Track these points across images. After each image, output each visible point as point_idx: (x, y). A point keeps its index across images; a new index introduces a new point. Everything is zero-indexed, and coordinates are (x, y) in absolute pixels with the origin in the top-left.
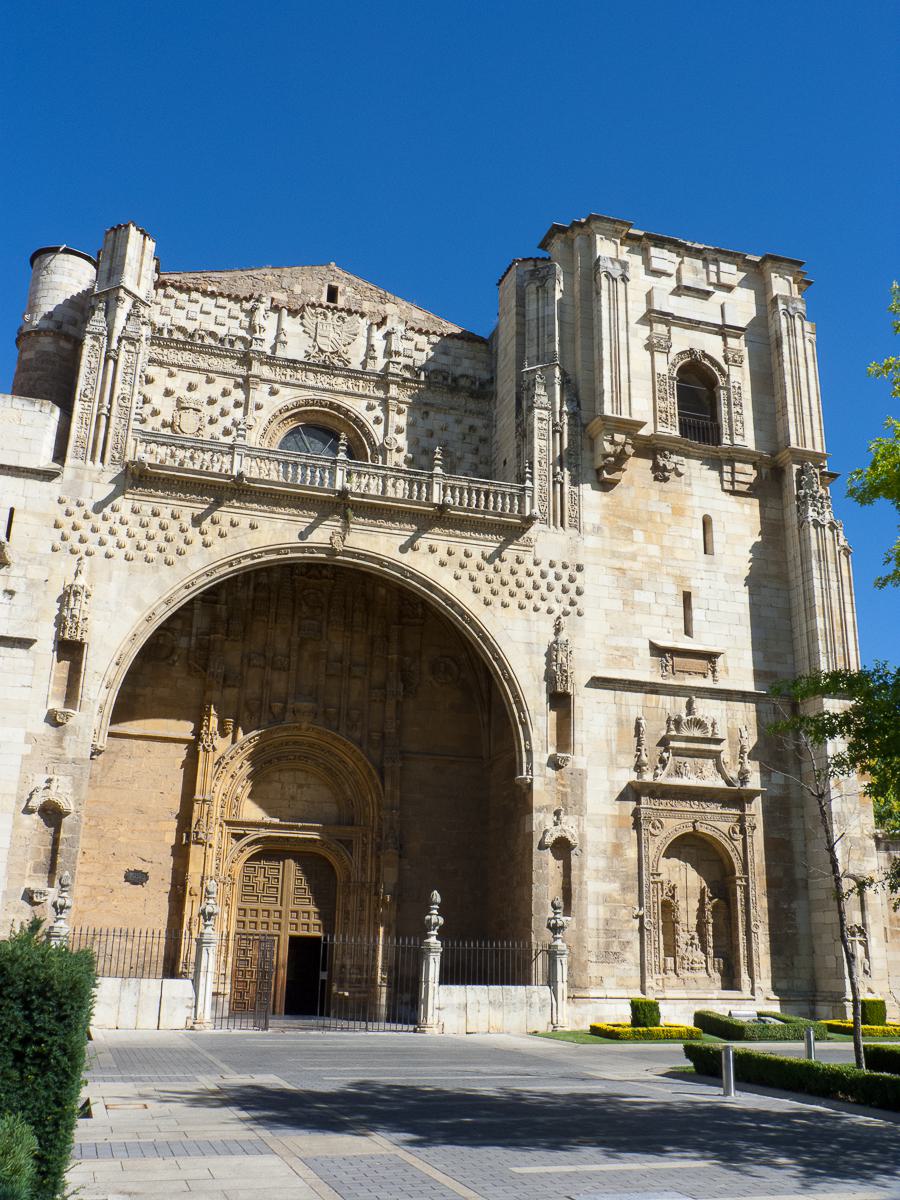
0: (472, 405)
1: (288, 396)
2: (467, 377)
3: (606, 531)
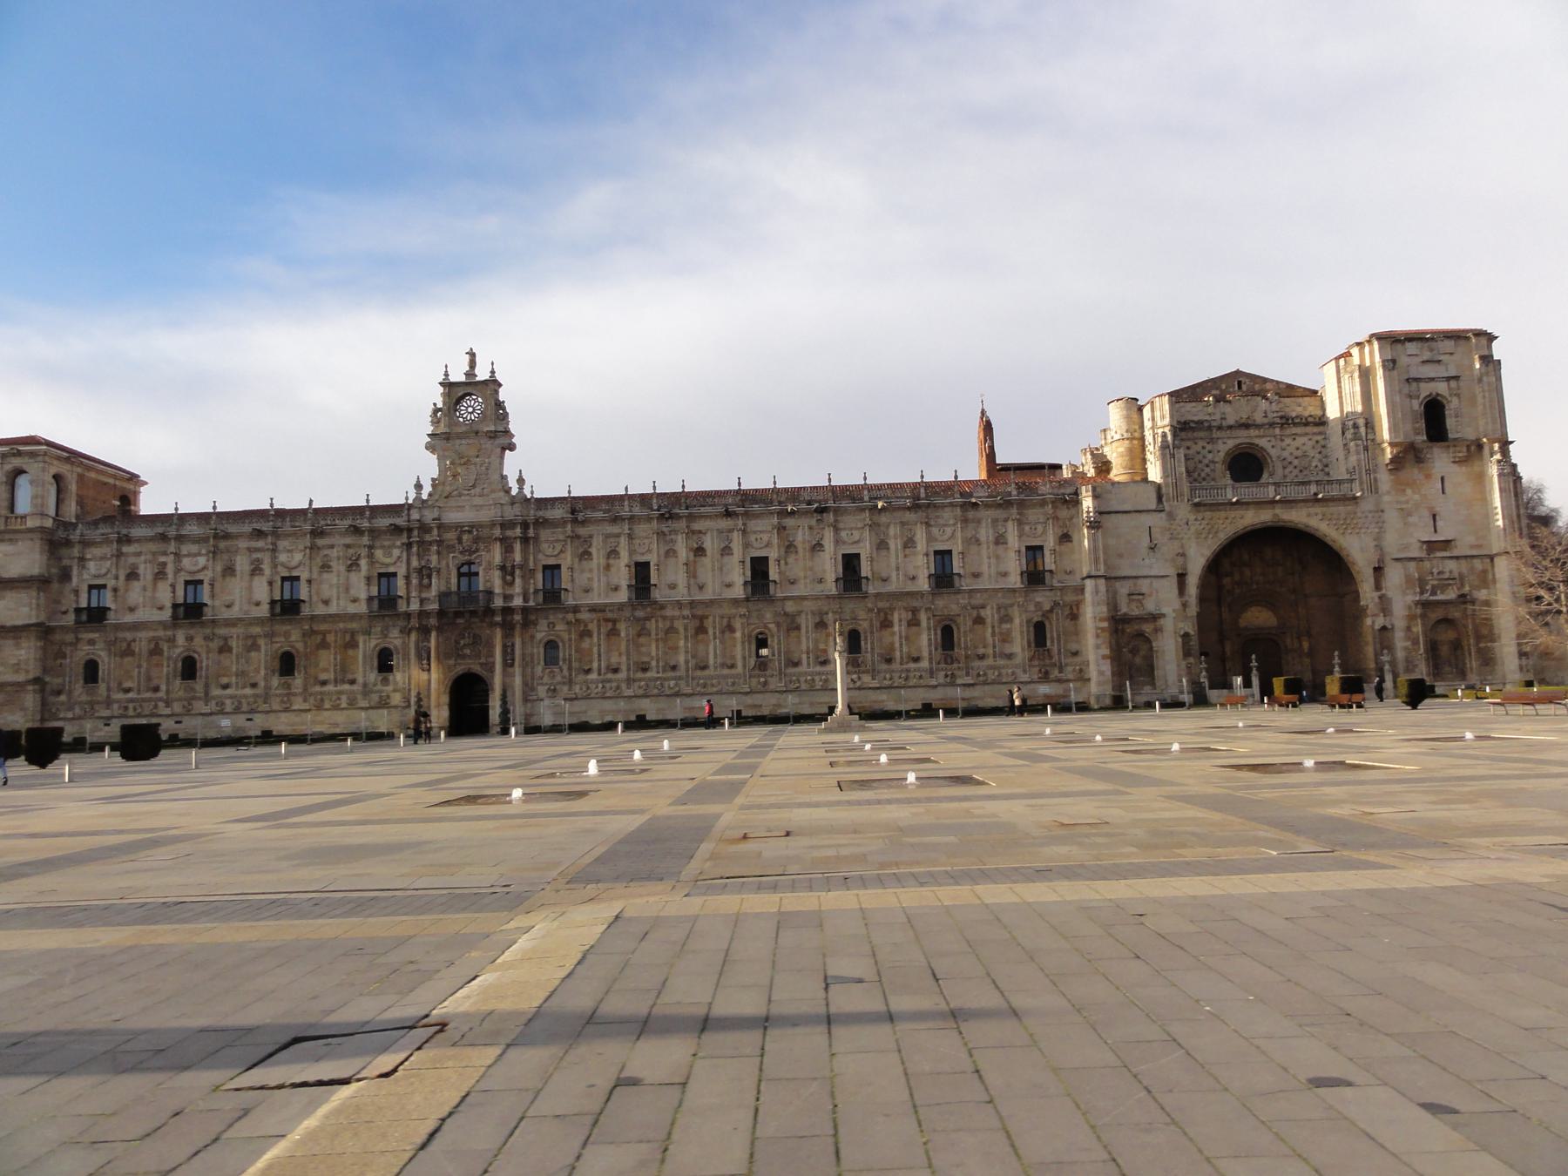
0: (1316, 429)
1: (1231, 443)
2: (1311, 416)
3: (1393, 493)
